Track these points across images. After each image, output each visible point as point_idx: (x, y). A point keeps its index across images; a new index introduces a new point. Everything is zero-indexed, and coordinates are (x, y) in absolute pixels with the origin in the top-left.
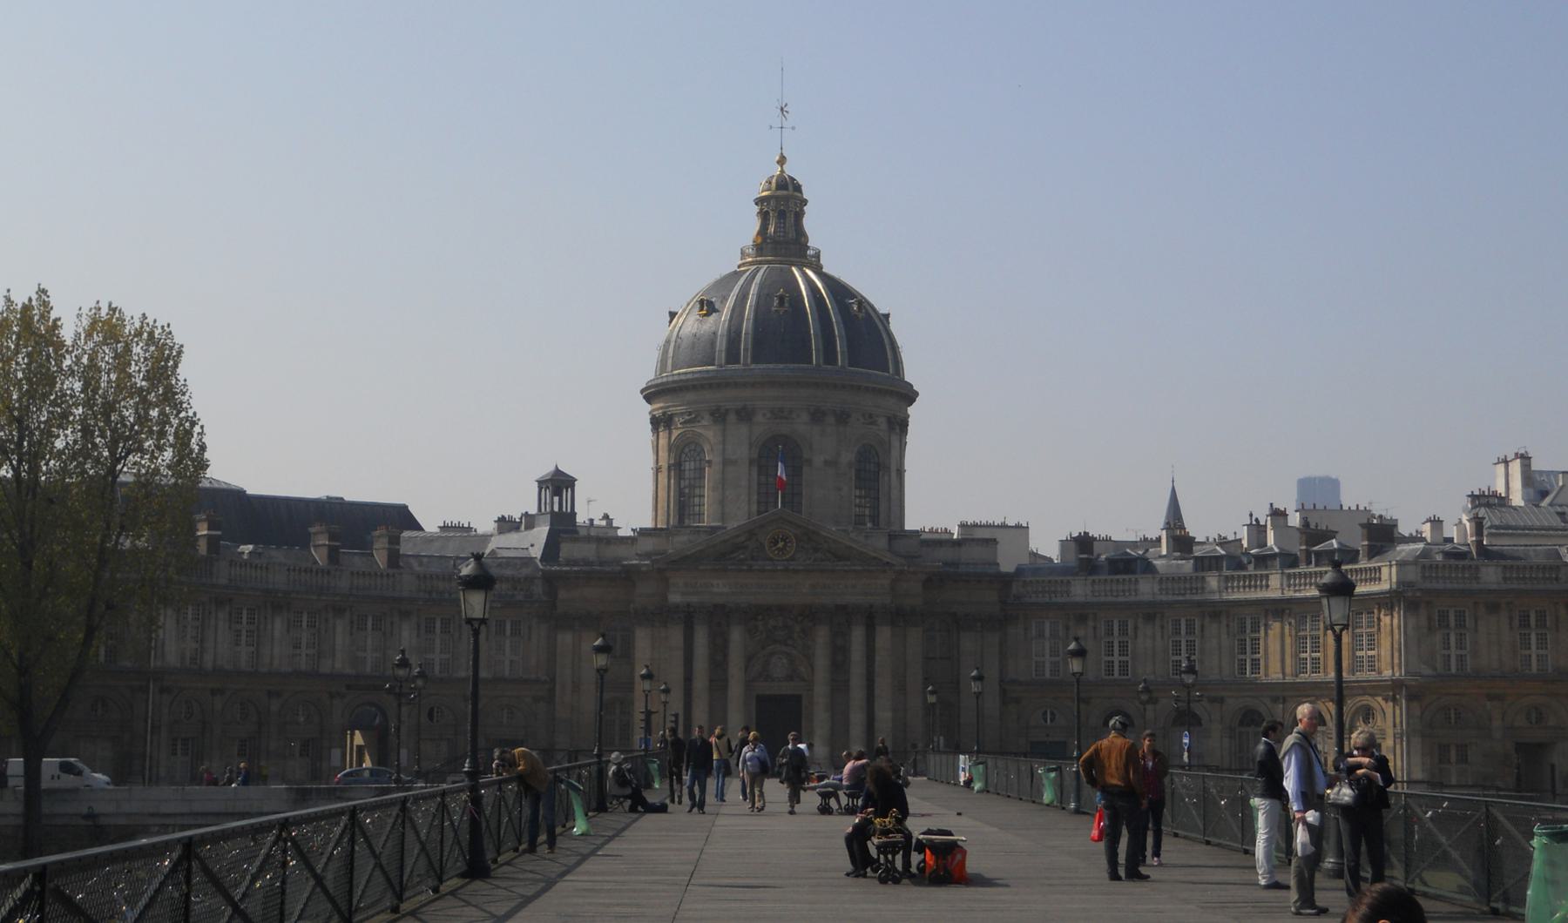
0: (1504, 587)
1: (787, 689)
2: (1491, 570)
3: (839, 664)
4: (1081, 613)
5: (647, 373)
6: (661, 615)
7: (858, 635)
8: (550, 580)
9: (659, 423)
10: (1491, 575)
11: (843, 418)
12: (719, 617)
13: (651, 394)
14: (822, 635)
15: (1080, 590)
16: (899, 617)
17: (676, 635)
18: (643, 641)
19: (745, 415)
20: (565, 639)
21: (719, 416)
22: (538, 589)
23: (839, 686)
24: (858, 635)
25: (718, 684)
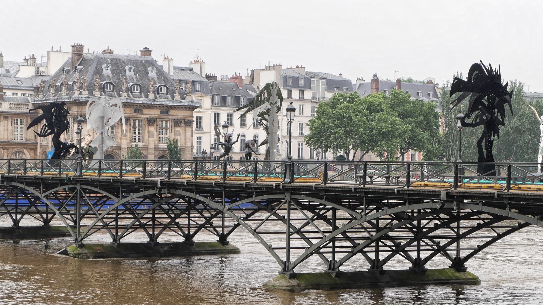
0: (10, 111)
2: (6, 104)
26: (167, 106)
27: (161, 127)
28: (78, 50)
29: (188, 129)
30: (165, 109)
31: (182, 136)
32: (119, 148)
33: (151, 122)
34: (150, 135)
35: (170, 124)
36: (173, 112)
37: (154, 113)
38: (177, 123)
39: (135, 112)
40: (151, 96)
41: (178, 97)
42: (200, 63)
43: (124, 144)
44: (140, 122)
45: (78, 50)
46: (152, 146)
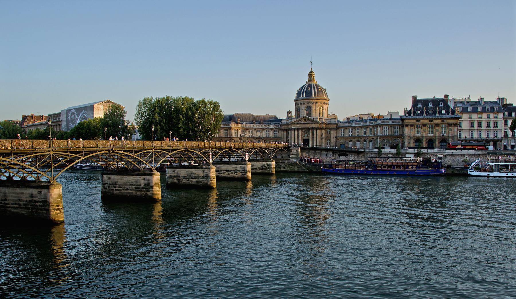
1: (307, 138)
3: (313, 135)
4: (346, 128)
5: (294, 97)
6: (291, 129)
7: (315, 131)
8: (281, 125)
9: (296, 105)
10: (391, 122)
11: (316, 103)
12: (298, 129)
13: (295, 101)
14: (311, 131)
15: (346, 125)
16: (321, 129)
17: (293, 132)
18: (289, 132)
19: (304, 104)
20: (283, 132)
21: (301, 104)
22: (279, 126)
23: (313, 138)
24: (315, 131)
25: (298, 138)
26: (444, 118)
27: (442, 127)
28: (414, 98)
29: (456, 128)
30: (443, 120)
31: (453, 131)
32: (422, 136)
33: (437, 125)
34: (437, 130)
35: (446, 125)
36: (448, 121)
37: (439, 121)
38: (450, 125)
39: (430, 121)
40: (437, 115)
41: (450, 114)
42: (503, 99)
43: (424, 135)
44: (432, 126)
45: (414, 98)
46: (437, 135)
